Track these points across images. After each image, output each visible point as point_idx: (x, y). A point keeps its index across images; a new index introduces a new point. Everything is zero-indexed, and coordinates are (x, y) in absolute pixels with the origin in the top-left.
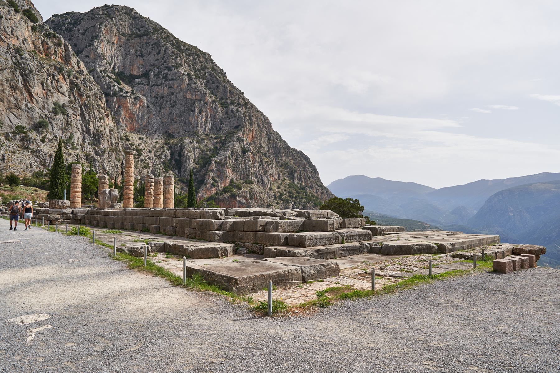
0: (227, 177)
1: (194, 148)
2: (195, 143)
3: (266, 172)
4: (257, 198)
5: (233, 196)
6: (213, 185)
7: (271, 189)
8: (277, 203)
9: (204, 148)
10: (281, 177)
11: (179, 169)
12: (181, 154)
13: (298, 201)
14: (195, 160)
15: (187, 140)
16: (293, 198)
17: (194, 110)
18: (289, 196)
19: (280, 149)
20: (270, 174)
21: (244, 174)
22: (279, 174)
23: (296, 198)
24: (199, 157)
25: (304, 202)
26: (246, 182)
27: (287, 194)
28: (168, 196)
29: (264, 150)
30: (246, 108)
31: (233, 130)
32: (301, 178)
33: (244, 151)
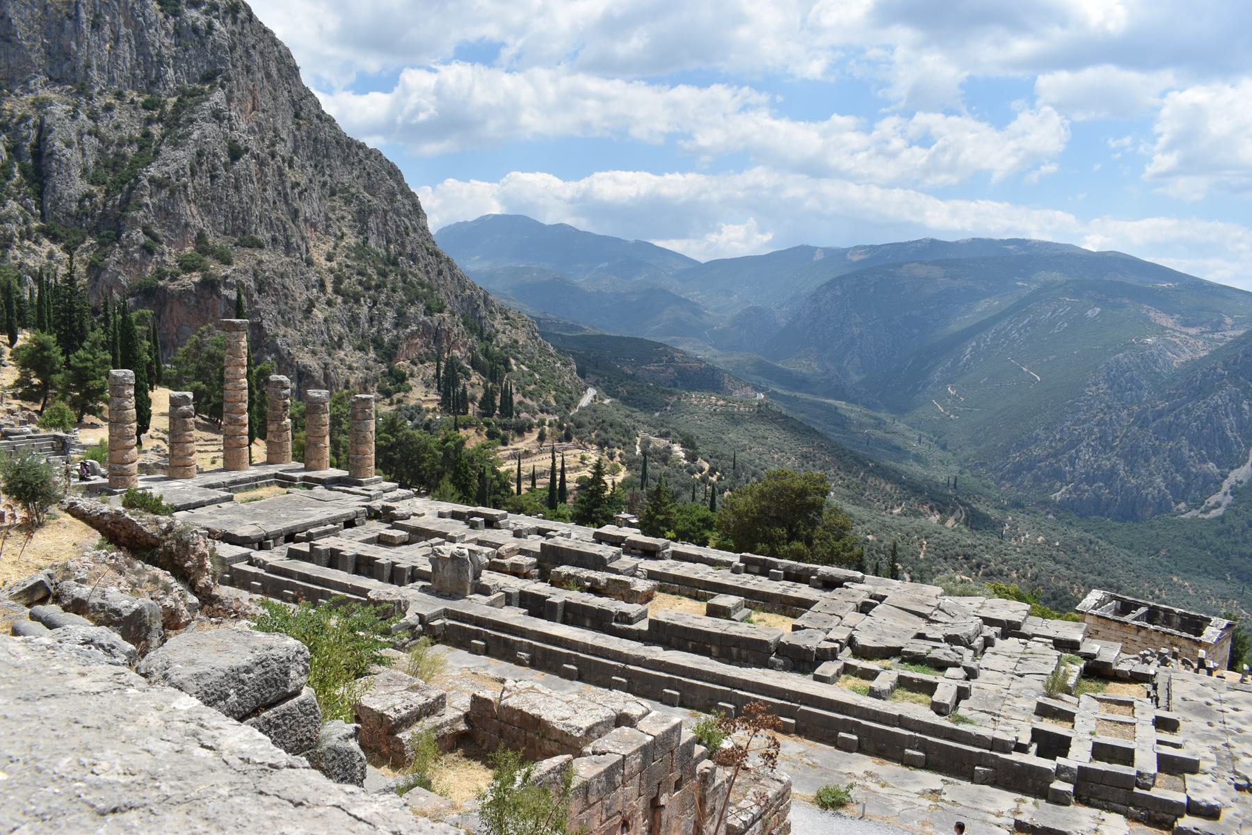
0: (187, 225)
1: (80, 134)
2: (83, 116)
3: (295, 214)
4: (275, 290)
5: (210, 285)
6: (148, 250)
7: (309, 263)
8: (330, 303)
9: (114, 136)
10: (334, 229)
11: (40, 195)
12: (41, 152)
13: (383, 297)
14: (85, 171)
15: (59, 109)
16: (368, 288)
17: (77, 13)
18: (360, 283)
19: (326, 144)
20: (306, 220)
21: (235, 219)
22: (328, 219)
23: (378, 287)
24: (97, 163)
25: (401, 302)
26: (242, 244)
27: (355, 277)
28: (361, 448)
29: (282, 149)
30: (235, 22)
31: (198, 86)
32: (387, 232)
33: (235, 153)
